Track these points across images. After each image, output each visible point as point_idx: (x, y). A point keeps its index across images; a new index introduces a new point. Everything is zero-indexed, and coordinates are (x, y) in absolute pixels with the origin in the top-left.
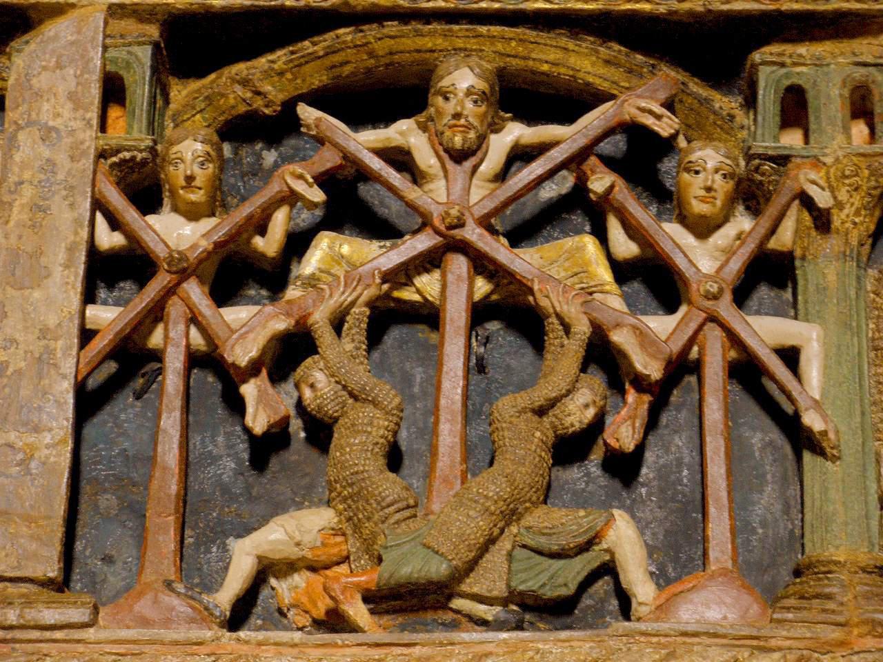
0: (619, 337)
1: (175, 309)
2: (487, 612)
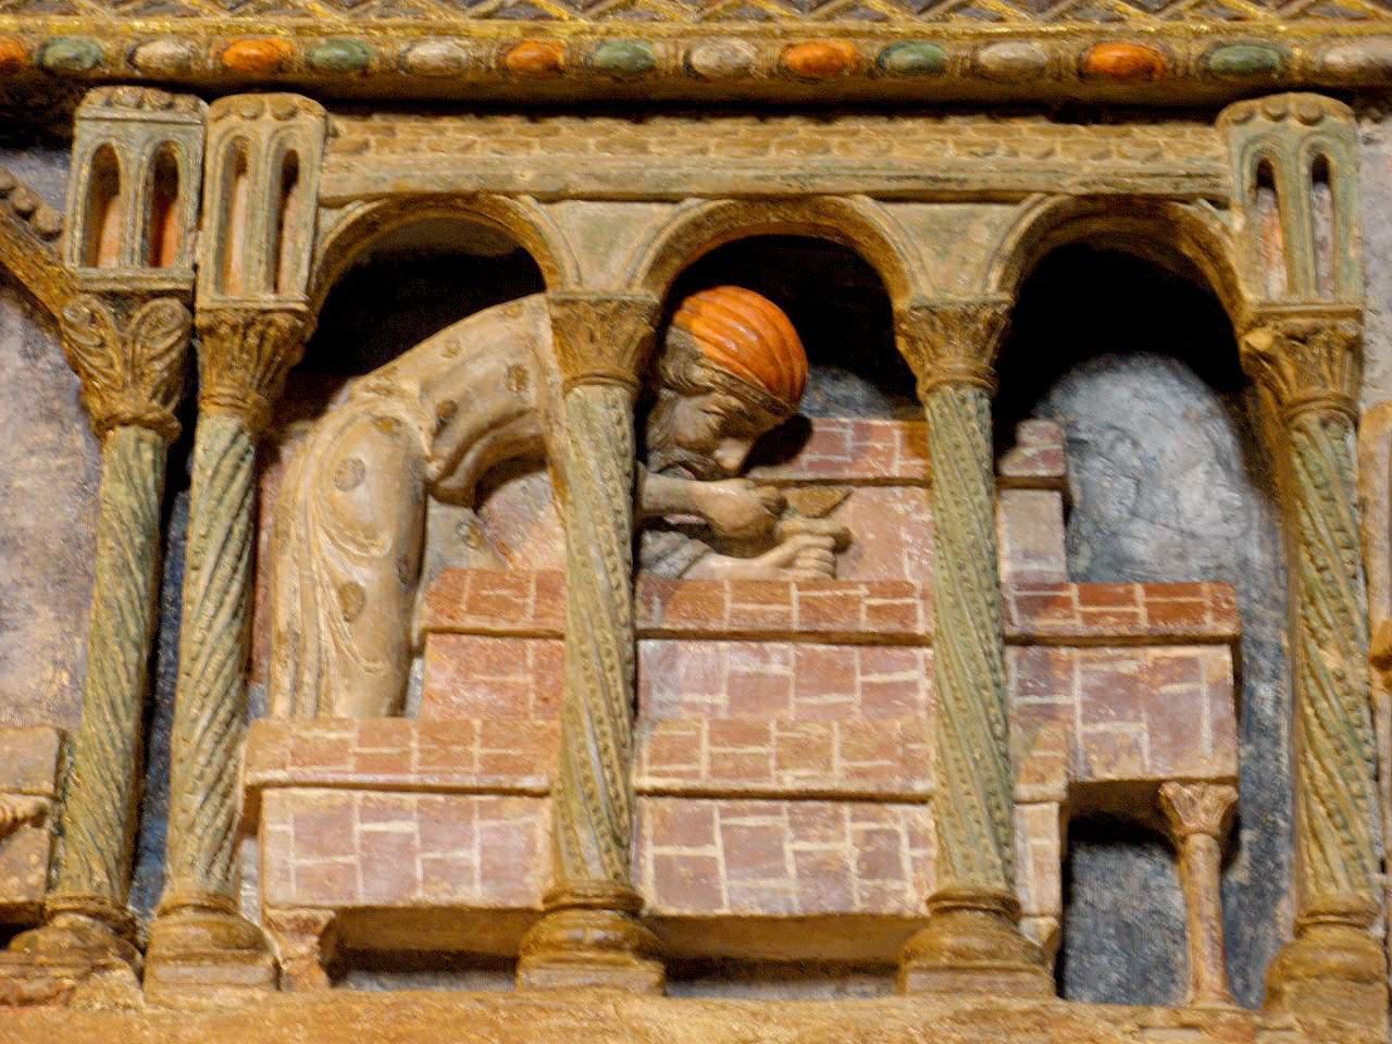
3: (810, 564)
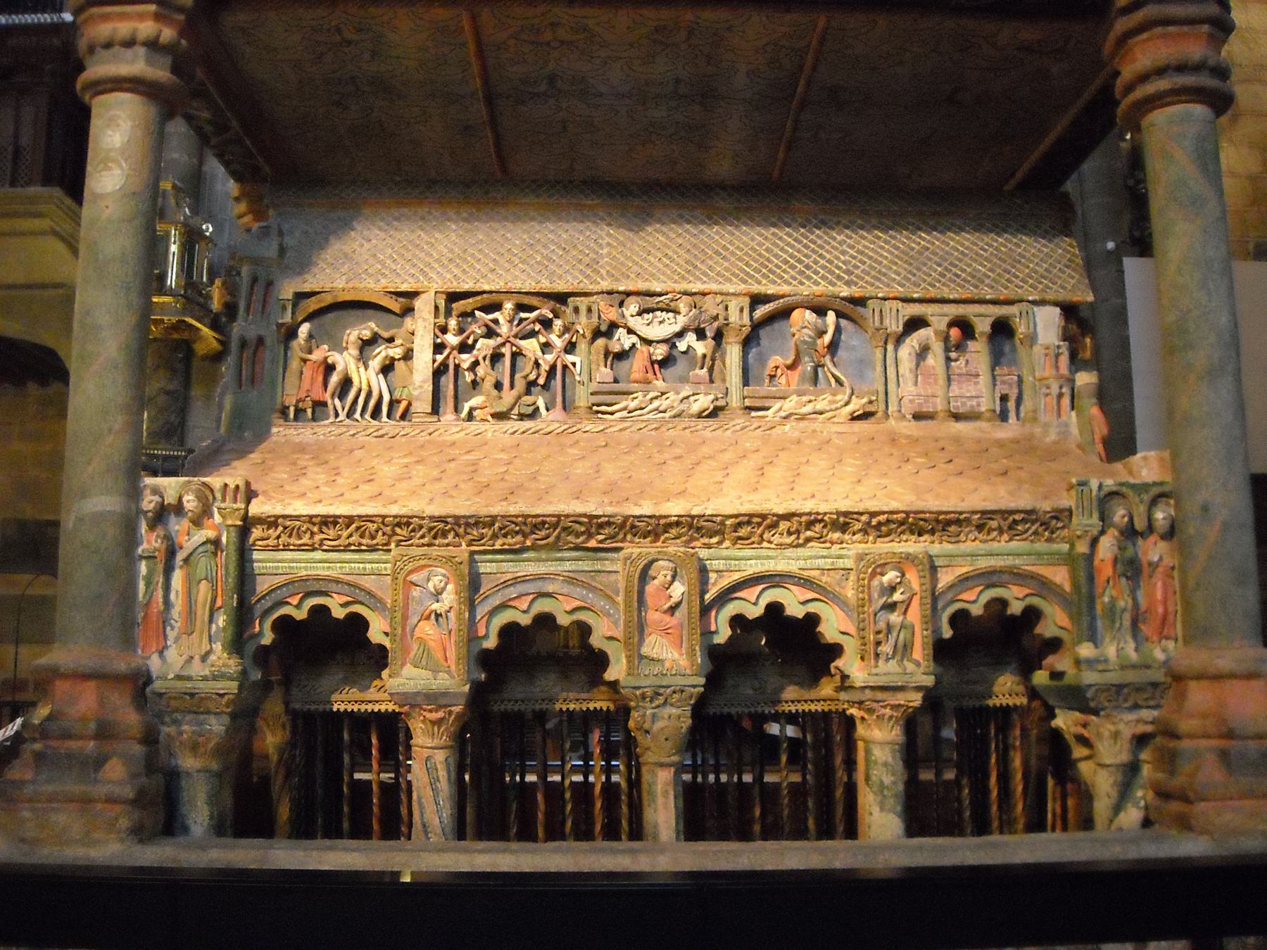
0: (540, 361)
1: (451, 357)
2: (515, 417)
3: (963, 365)
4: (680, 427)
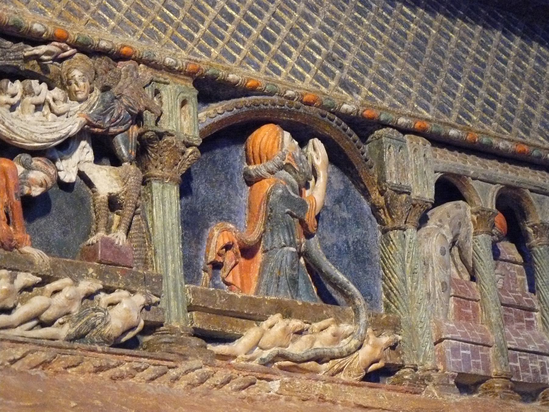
4: (88, 366)
